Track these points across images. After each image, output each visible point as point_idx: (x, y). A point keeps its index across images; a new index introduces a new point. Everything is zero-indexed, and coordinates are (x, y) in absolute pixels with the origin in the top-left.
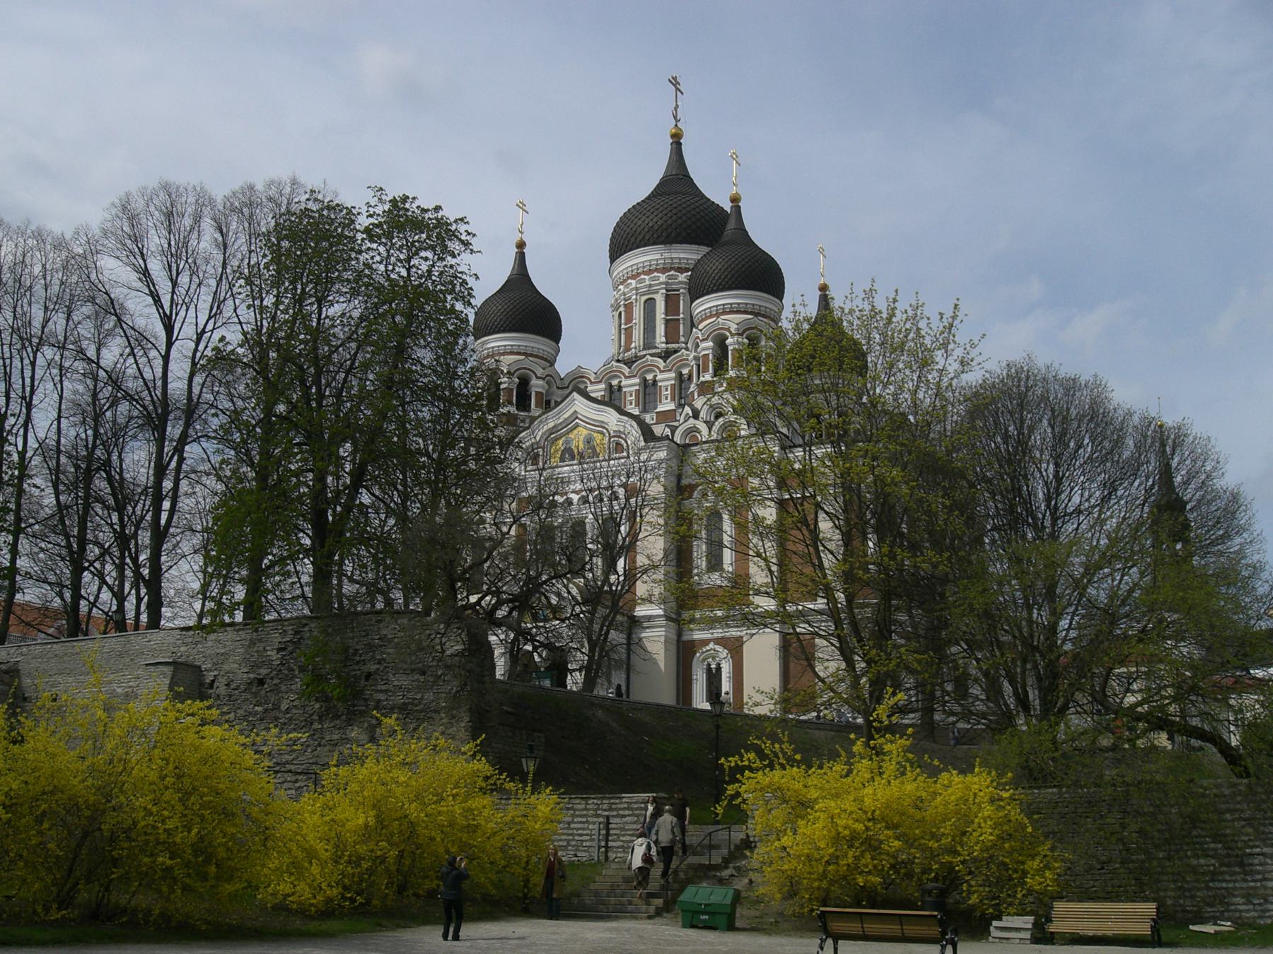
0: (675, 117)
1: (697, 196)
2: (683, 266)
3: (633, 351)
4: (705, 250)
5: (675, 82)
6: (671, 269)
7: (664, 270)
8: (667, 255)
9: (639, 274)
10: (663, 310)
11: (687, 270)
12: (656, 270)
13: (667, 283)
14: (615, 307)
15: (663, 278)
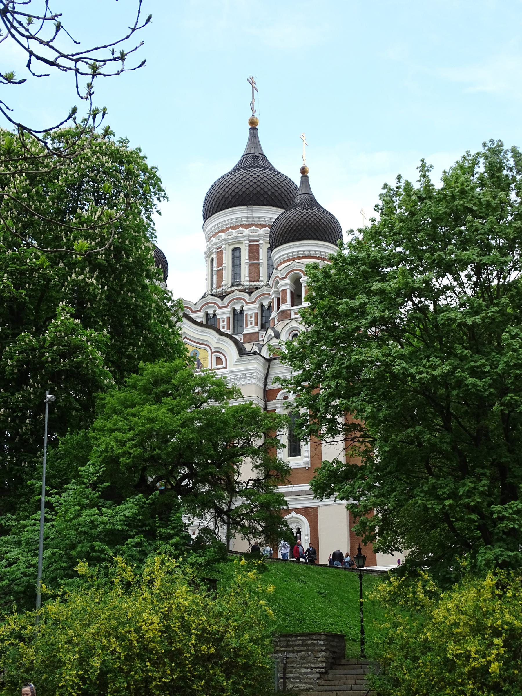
0: (252, 108)
1: (271, 169)
2: (262, 223)
3: (224, 287)
4: (282, 211)
5: (251, 81)
6: (253, 225)
7: (247, 226)
8: (250, 214)
9: (227, 229)
10: (247, 257)
11: (264, 226)
12: (242, 226)
13: (248, 236)
14: (208, 254)
15: (246, 232)
